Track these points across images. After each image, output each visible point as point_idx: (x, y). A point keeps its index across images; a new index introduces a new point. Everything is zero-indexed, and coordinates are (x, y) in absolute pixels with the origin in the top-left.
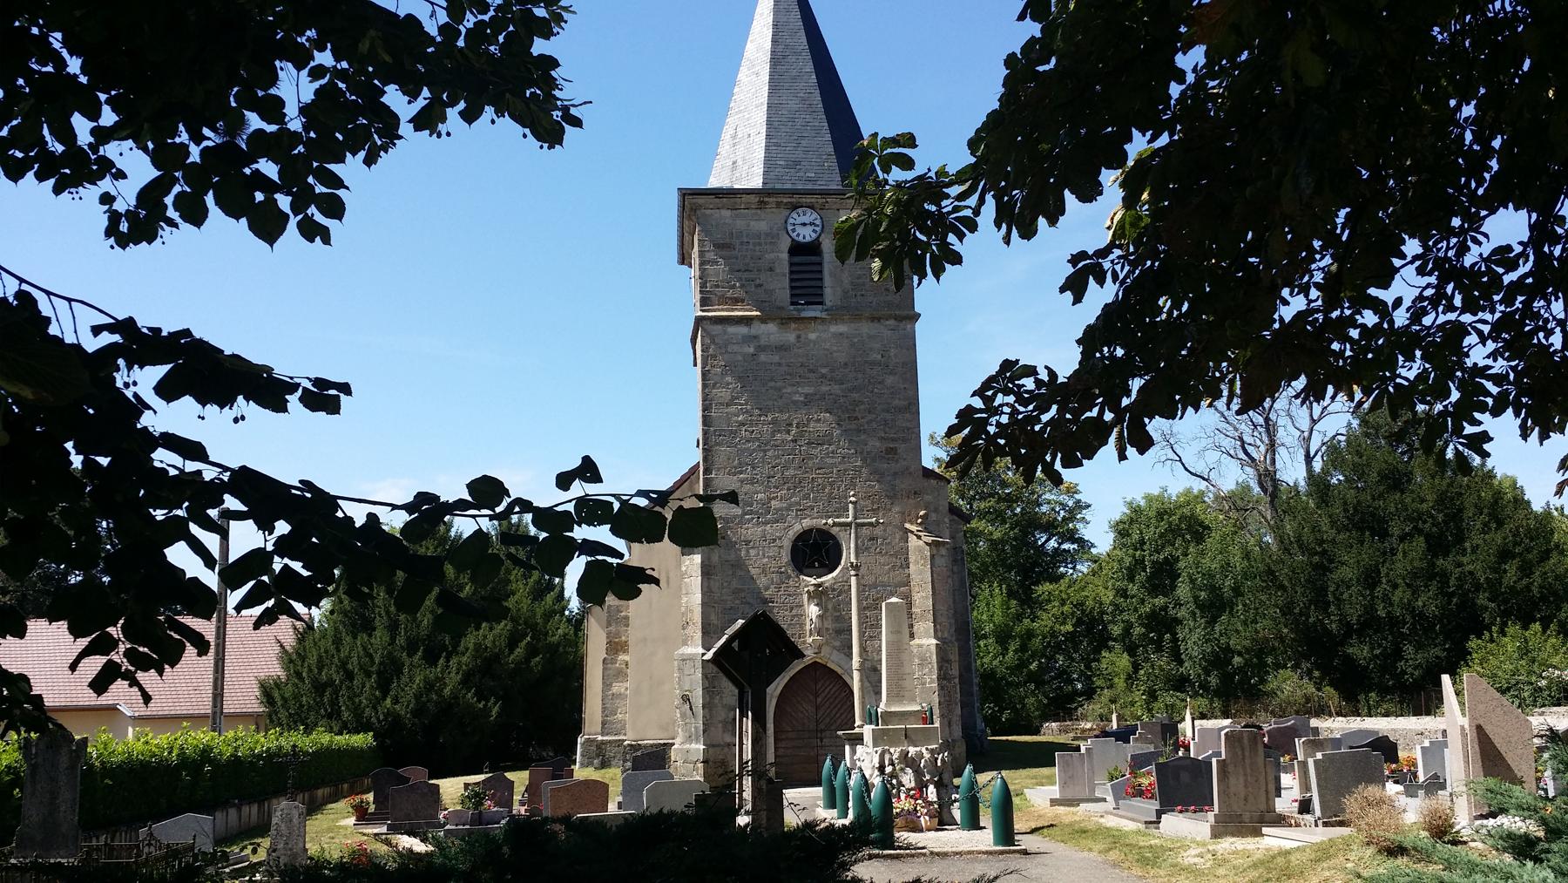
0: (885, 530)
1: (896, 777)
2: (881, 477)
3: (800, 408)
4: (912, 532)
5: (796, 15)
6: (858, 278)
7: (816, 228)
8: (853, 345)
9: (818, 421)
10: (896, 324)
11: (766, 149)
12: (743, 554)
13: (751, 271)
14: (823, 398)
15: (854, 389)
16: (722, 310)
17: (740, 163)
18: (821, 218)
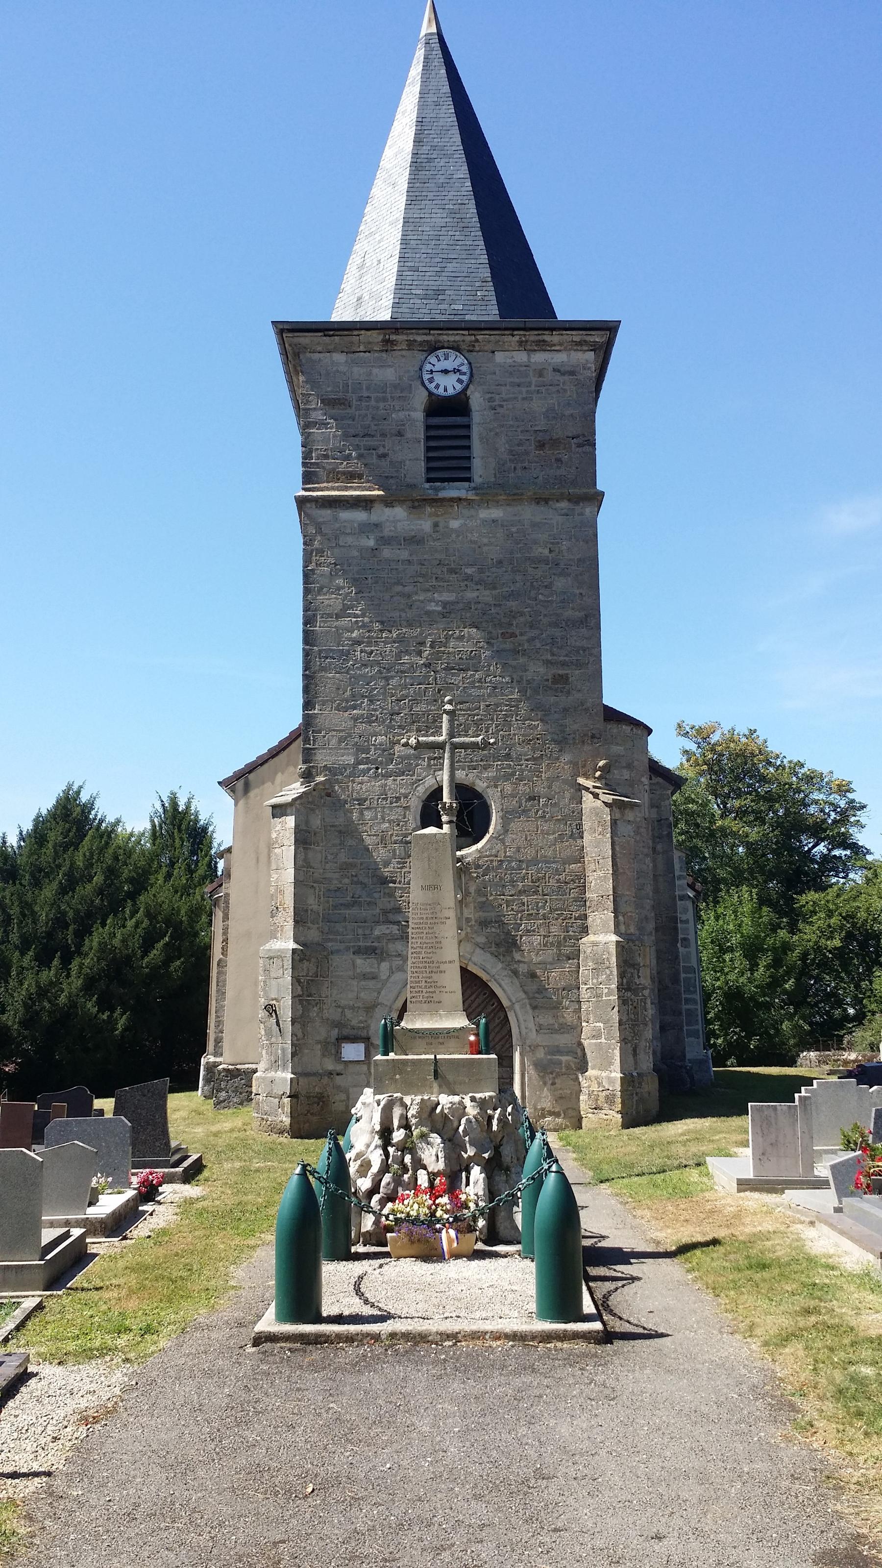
0: (550, 787)
1: (412, 1151)
2: (545, 715)
3: (437, 622)
4: (587, 789)
5: (448, 113)
6: (518, 445)
7: (462, 377)
8: (510, 535)
9: (461, 638)
10: (571, 506)
11: (398, 275)
12: (355, 815)
13: (373, 436)
14: (468, 607)
15: (512, 595)
16: (333, 489)
17: (367, 298)
18: (470, 363)
